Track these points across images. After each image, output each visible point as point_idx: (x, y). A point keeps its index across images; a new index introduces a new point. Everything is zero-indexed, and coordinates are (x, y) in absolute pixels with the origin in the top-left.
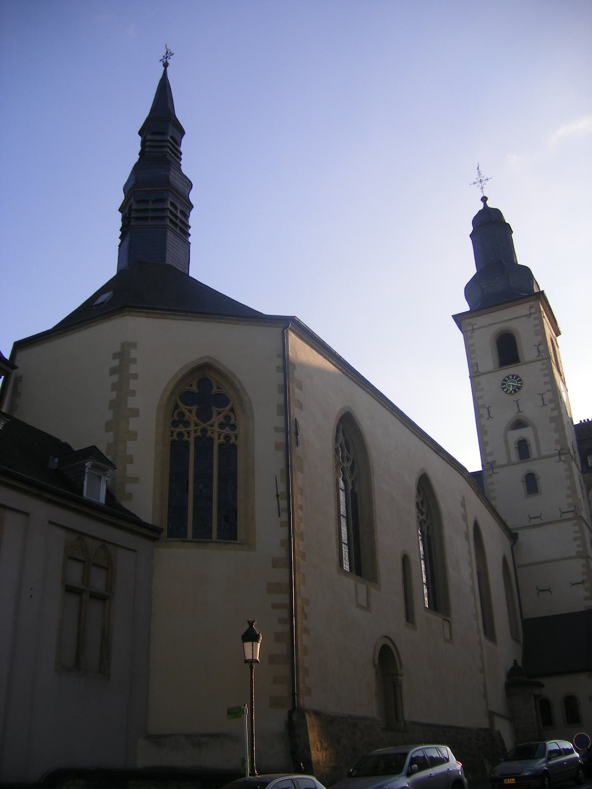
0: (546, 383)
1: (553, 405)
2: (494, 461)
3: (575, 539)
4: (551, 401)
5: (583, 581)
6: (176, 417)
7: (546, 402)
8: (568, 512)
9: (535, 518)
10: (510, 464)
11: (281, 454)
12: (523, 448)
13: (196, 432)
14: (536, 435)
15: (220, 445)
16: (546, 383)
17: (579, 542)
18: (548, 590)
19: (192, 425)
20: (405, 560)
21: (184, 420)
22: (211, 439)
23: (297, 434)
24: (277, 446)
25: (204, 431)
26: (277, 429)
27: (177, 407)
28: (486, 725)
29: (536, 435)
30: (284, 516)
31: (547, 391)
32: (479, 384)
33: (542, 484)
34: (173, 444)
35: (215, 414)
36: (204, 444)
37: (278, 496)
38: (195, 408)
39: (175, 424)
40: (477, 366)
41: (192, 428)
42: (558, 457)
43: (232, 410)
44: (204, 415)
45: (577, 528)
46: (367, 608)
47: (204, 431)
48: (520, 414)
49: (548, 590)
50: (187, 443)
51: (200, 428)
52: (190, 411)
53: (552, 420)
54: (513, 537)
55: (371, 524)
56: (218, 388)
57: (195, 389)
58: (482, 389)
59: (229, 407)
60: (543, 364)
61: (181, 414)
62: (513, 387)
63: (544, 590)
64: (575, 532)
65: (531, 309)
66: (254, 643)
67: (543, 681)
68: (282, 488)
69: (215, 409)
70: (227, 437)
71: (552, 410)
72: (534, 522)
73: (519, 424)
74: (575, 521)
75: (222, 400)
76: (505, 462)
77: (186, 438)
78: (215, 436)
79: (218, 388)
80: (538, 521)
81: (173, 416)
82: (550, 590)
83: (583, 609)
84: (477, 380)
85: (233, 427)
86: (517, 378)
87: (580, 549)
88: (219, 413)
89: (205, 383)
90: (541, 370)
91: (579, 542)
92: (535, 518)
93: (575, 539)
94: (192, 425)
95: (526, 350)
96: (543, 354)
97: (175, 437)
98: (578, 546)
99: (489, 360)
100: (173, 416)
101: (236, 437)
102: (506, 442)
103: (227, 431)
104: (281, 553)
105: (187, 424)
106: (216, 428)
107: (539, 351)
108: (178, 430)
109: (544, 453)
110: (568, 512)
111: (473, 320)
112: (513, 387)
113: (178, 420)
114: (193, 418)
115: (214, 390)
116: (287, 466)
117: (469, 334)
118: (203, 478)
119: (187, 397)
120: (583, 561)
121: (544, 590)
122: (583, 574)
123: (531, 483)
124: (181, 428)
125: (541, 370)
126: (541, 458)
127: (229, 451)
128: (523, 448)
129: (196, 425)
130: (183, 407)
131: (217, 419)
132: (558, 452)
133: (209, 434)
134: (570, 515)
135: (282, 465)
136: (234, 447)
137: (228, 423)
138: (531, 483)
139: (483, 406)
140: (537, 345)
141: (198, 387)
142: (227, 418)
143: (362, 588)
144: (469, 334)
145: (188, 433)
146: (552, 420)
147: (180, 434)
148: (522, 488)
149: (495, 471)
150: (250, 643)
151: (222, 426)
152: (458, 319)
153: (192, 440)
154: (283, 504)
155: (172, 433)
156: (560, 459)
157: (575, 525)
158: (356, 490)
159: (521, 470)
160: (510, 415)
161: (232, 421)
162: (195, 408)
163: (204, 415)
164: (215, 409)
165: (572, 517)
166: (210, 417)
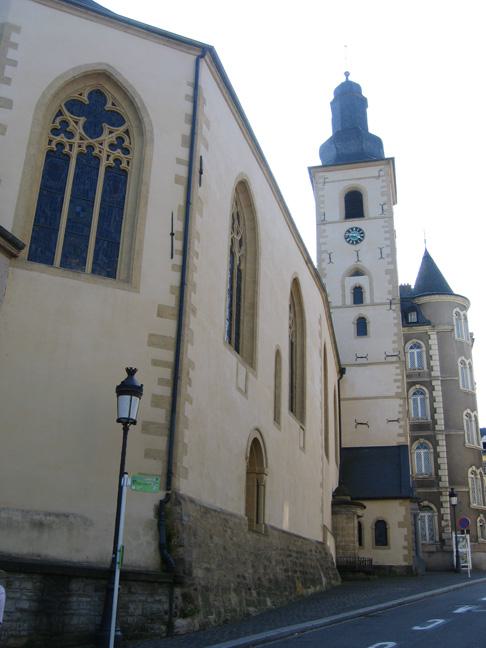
0: (386, 239)
1: (390, 260)
3: (396, 381)
4: (388, 256)
6: (57, 125)
10: (344, 306)
11: (181, 190)
12: (358, 295)
13: (80, 146)
15: (108, 168)
16: (386, 239)
17: (399, 384)
19: (77, 137)
20: (278, 353)
21: (68, 129)
22: (97, 159)
23: (201, 173)
24: (177, 180)
25: (90, 147)
26: (179, 161)
27: (60, 113)
28: (321, 540)
30: (178, 259)
31: (388, 246)
32: (324, 231)
33: (371, 328)
34: (50, 154)
35: (106, 132)
36: (88, 162)
37: (172, 234)
38: (82, 120)
39: (55, 132)
41: (76, 140)
43: (127, 132)
44: (93, 130)
45: (398, 371)
46: (245, 393)
47: (90, 147)
50: (68, 157)
51: (85, 143)
52: (76, 123)
53: (388, 272)
54: (342, 371)
55: (254, 306)
56: (113, 104)
57: (85, 99)
59: (122, 128)
61: (65, 123)
62: (355, 238)
64: (397, 375)
66: (134, 398)
67: (365, 503)
68: (179, 227)
69: (106, 127)
70: (118, 161)
71: (389, 263)
72: (360, 361)
73: (357, 273)
74: (397, 365)
75: (117, 119)
76: (340, 304)
77: (67, 149)
78: (104, 156)
79: (113, 104)
80: (364, 361)
81: (54, 122)
83: (395, 444)
84: (323, 227)
85: (126, 151)
86: (360, 230)
87: (400, 390)
88: (111, 132)
89: (98, 96)
90: (383, 227)
91: (399, 384)
93: (396, 381)
94: (77, 137)
95: (371, 205)
97: (53, 146)
98: (398, 387)
99: (337, 209)
100: (54, 122)
101: (128, 163)
102: (343, 287)
103: (118, 153)
104: (171, 301)
105: (70, 135)
106: (106, 147)
108: (58, 138)
109: (376, 301)
111: (327, 174)
112: (355, 238)
113: (62, 129)
114: (79, 130)
115: (109, 106)
116: (188, 203)
117: (320, 186)
118: (83, 196)
119: (73, 105)
120: (401, 402)
122: (400, 412)
123: (362, 327)
124: (62, 138)
125: (383, 227)
126: (373, 304)
127: (118, 178)
128: (358, 295)
129: (81, 139)
130: (68, 116)
131: (107, 138)
133: (96, 151)
134: (394, 359)
135: (181, 201)
136: (125, 173)
137: (118, 144)
138: (362, 327)
139: (326, 251)
141: (89, 97)
142: (120, 139)
143: (243, 370)
144: (320, 186)
145: (71, 146)
146: (388, 272)
147: (60, 145)
148: (353, 329)
150: (128, 397)
151: (112, 146)
152: (312, 171)
153: (74, 155)
154: (178, 245)
155: (50, 141)
157: (397, 368)
158: (242, 267)
159: (356, 312)
160: (350, 263)
161: (126, 143)
162: (82, 120)
163: (93, 130)
164: (106, 127)
166: (100, 134)
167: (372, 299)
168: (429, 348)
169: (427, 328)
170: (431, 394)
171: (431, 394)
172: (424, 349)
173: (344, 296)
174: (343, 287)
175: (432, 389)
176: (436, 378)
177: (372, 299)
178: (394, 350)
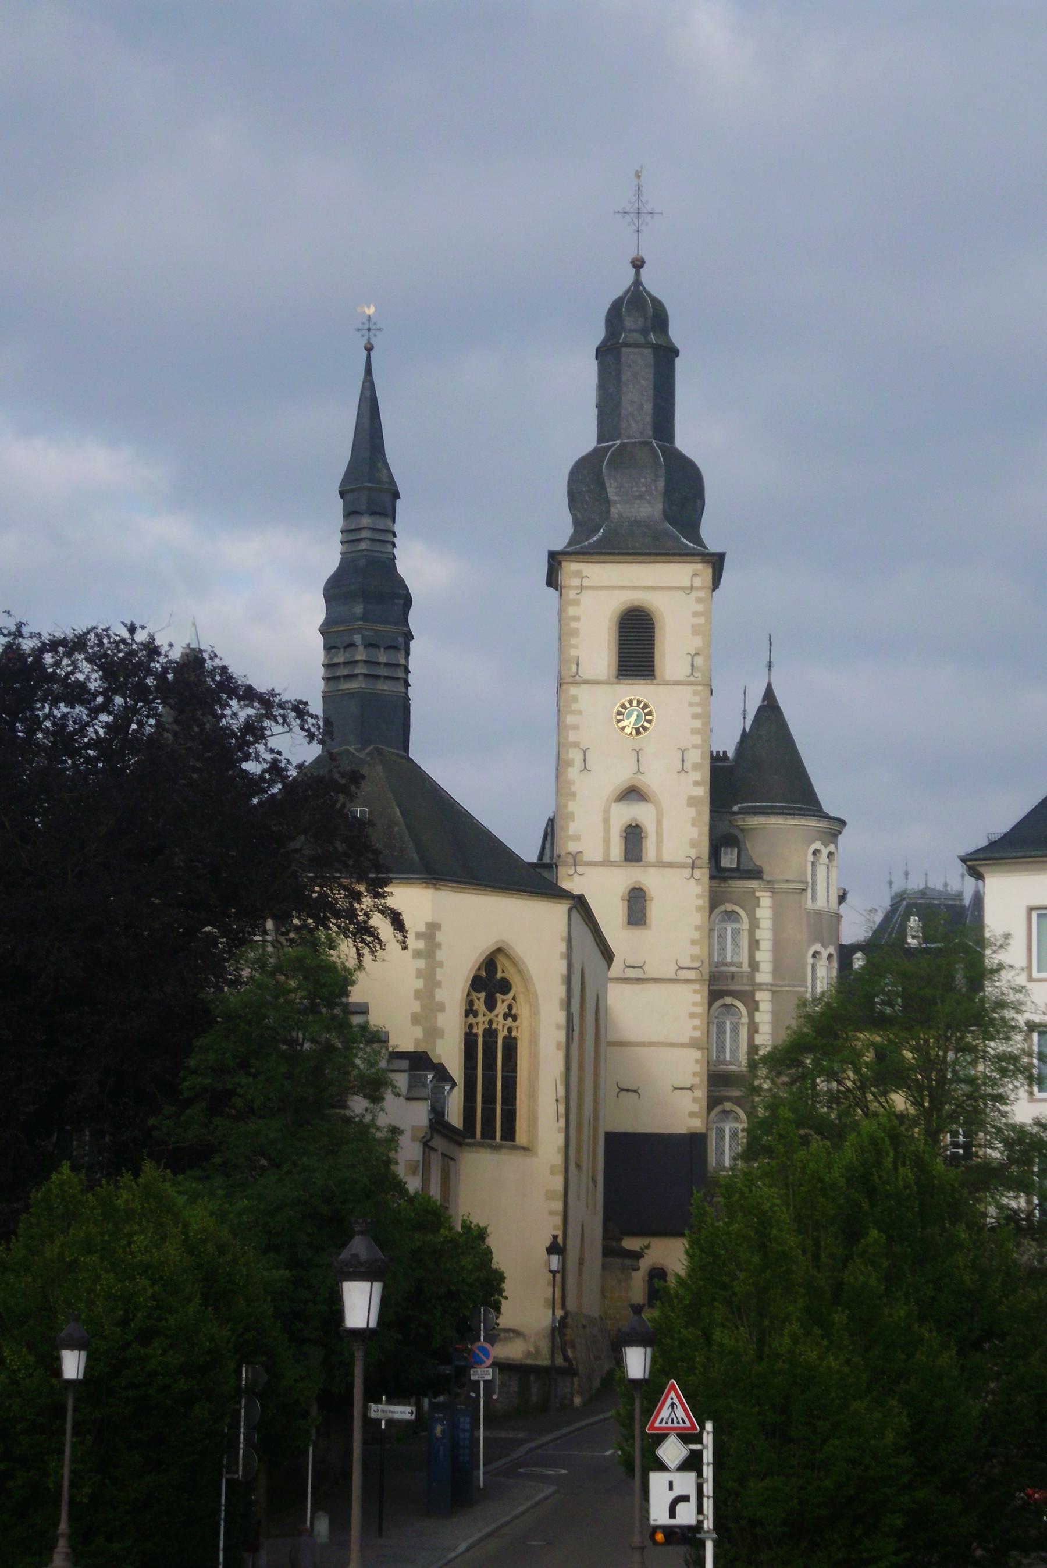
2: (581, 852)
3: (692, 1016)
5: (692, 1086)
7: (688, 765)
8: (689, 968)
9: (634, 967)
10: (607, 863)
14: (659, 823)
18: (635, 1091)
29: (659, 823)
31: (695, 747)
40: (578, 665)
42: (690, 870)
48: (639, 776)
49: (635, 1091)
58: (580, 713)
60: (695, 693)
63: (628, 1090)
65: (693, 578)
76: (598, 856)
82: (639, 1091)
92: (634, 967)
93: (692, 1016)
96: (699, 674)
102: (606, 821)
107: (692, 665)
109: (667, 858)
110: (689, 968)
121: (628, 1090)
132: (691, 861)
140: (693, 654)
149: (580, 869)
156: (692, 876)
165: (694, 978)
167: (659, 853)
168: (754, 924)
169: (754, 884)
170: (751, 1017)
171: (751, 1017)
172: (746, 925)
173: (607, 842)
174: (606, 821)
175: (753, 1007)
176: (761, 987)
177: (659, 853)
178: (693, 957)
